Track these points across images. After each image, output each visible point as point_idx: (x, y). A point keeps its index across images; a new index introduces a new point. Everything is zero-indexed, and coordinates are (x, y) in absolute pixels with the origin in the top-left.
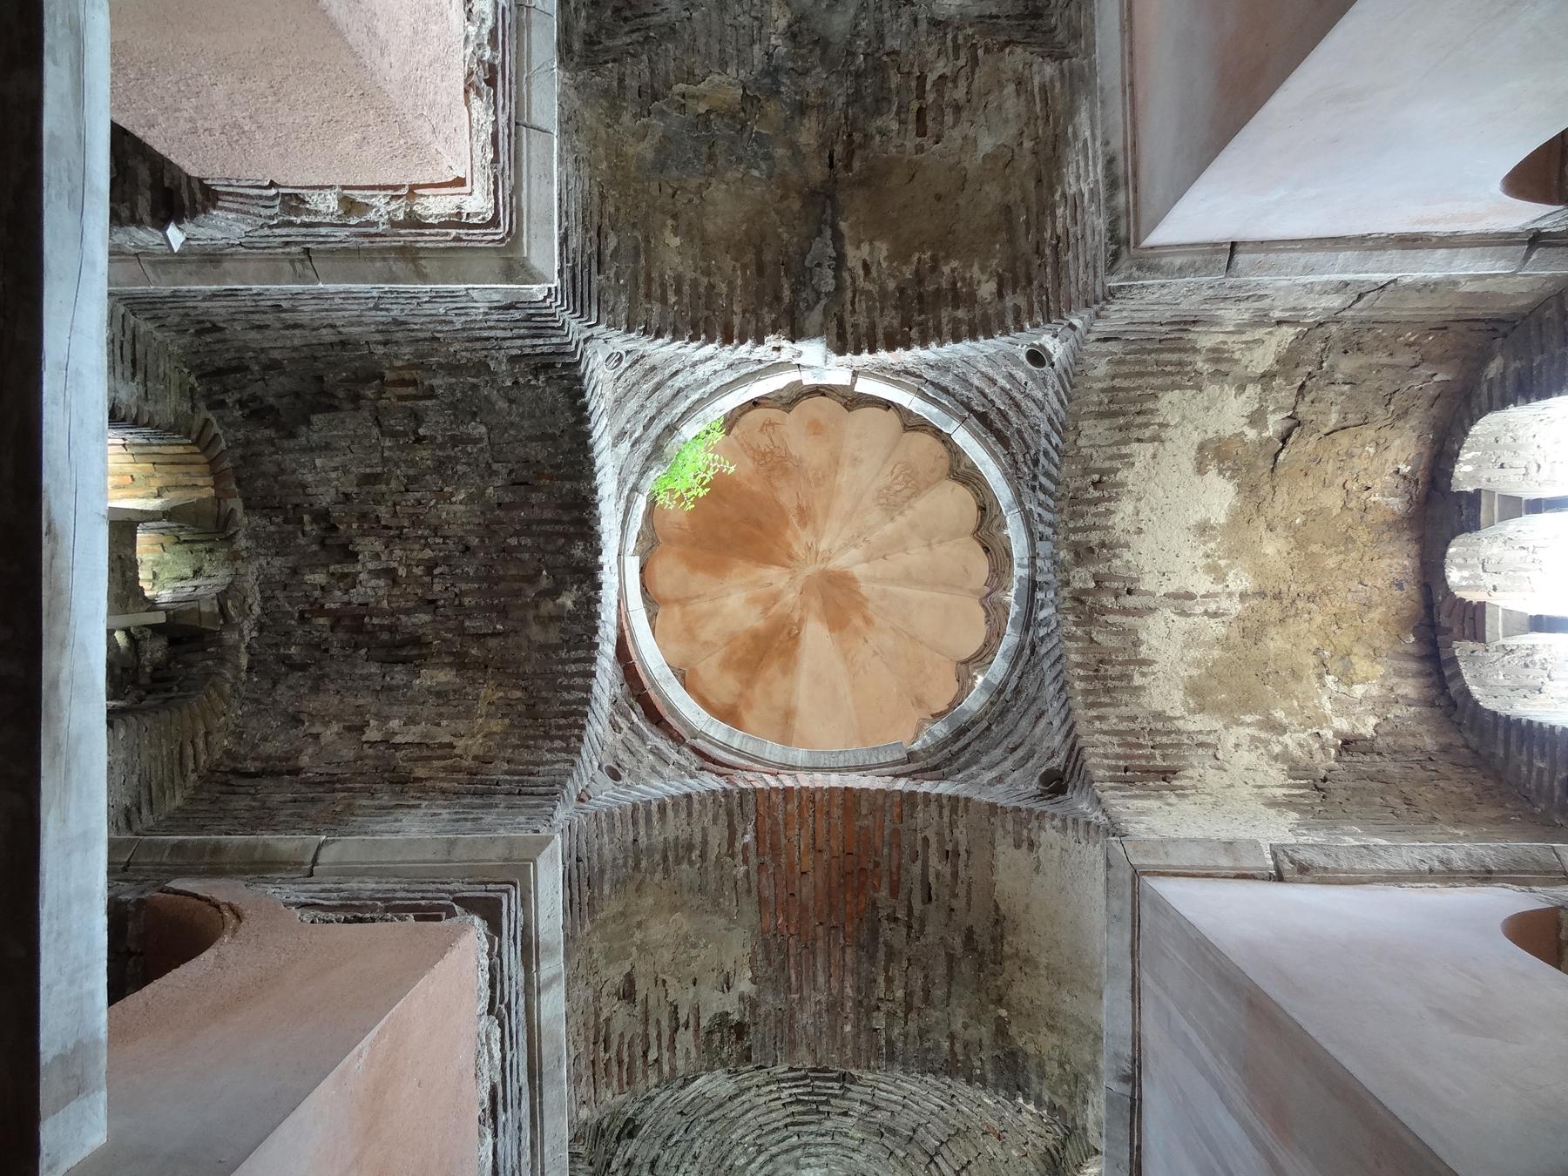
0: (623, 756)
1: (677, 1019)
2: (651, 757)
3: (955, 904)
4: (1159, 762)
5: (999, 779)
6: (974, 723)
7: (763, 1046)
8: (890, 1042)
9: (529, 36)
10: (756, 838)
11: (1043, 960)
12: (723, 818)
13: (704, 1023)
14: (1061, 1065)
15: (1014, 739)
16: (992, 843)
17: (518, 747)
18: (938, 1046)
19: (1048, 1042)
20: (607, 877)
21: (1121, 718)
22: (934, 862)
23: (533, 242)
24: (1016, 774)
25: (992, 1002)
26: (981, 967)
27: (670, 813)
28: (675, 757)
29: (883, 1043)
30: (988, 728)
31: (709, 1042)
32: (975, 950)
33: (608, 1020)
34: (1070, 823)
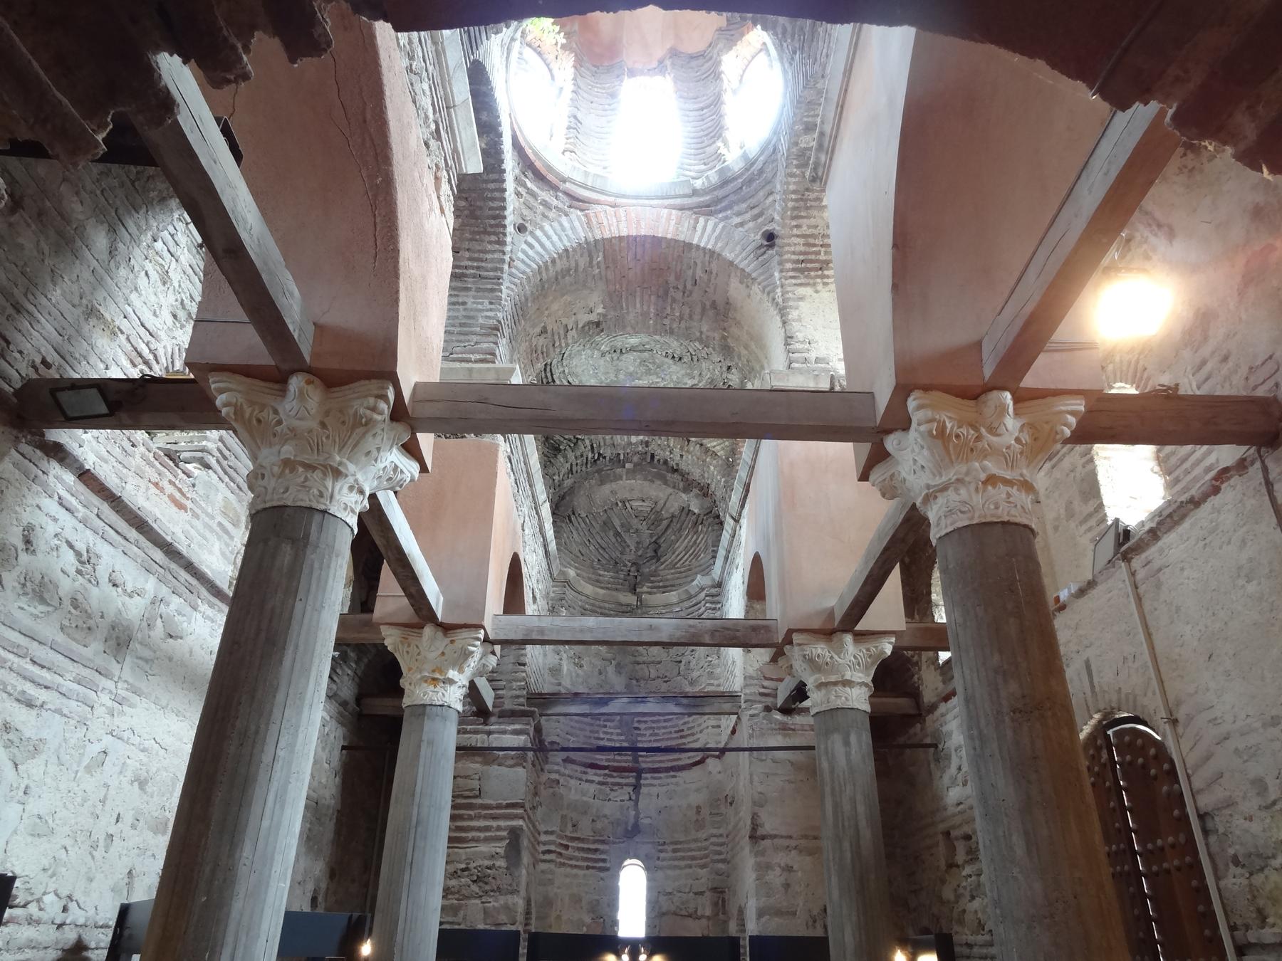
0: (526, 212)
2: (541, 207)
3: (707, 290)
4: (822, 257)
5: (742, 224)
6: (735, 179)
7: (609, 328)
9: (445, 57)
10: (604, 257)
11: (746, 328)
12: (586, 255)
13: (580, 326)
14: (748, 361)
15: (752, 201)
16: (729, 276)
17: (471, 240)
19: (744, 352)
20: (530, 299)
21: (809, 227)
22: (699, 273)
23: (468, 163)
24: (751, 224)
26: (717, 314)
27: (558, 261)
28: (555, 202)
30: (741, 188)
32: (716, 308)
34: (769, 291)
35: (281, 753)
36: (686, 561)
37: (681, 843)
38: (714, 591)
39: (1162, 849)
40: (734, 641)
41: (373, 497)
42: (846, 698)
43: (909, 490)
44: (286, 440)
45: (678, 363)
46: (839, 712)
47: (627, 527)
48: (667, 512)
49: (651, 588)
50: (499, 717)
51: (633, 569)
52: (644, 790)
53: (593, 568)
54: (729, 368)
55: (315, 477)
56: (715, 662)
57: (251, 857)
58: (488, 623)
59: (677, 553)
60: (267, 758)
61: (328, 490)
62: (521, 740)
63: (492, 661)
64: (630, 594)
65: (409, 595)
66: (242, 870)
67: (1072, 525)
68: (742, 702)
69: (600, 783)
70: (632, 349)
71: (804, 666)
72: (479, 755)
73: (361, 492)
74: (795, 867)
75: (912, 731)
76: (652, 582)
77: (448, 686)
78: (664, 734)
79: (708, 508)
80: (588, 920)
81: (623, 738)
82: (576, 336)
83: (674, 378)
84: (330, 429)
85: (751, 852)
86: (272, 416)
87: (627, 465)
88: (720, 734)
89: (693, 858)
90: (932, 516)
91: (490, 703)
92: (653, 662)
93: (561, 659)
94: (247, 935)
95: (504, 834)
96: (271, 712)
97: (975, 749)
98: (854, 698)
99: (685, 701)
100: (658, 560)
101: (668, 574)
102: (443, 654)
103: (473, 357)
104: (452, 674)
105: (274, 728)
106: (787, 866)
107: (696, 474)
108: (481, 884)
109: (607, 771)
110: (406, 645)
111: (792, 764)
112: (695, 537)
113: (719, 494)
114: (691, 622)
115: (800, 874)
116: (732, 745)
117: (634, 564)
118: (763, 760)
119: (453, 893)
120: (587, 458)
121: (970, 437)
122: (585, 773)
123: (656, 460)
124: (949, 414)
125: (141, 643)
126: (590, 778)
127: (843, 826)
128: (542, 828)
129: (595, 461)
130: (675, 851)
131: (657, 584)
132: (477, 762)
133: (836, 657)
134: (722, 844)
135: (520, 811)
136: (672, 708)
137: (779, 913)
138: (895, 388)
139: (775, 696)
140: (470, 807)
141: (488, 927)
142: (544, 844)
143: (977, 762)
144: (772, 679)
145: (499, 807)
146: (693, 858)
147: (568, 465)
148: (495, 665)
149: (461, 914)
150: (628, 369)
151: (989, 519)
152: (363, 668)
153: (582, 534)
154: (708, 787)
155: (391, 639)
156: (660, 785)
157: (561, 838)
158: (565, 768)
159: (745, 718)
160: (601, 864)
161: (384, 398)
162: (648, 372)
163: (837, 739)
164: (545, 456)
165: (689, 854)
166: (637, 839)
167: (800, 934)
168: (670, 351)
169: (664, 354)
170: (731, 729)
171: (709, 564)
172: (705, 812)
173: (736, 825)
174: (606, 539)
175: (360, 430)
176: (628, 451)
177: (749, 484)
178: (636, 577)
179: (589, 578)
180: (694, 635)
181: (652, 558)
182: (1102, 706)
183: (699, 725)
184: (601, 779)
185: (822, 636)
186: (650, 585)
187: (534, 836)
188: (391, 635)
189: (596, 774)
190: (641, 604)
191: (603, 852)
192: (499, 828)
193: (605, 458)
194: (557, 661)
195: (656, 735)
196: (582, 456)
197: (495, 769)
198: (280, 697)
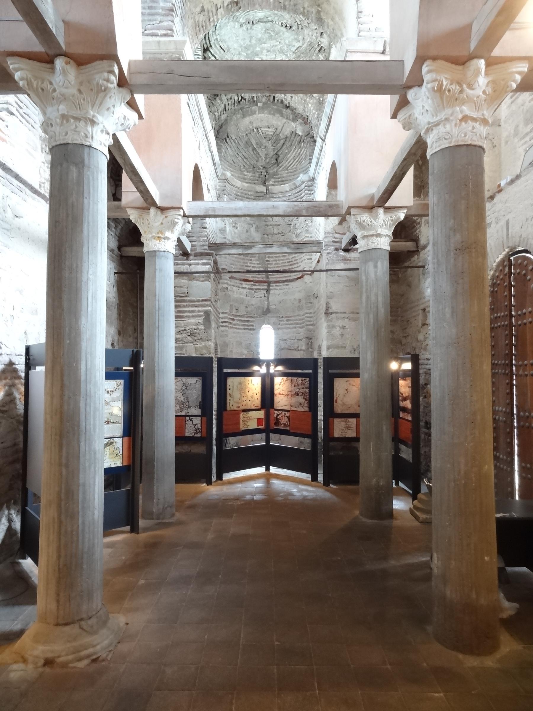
7: (244, 6)
8: (284, 5)
13: (226, 5)
14: (333, 30)
18: (300, 9)
19: (331, 23)
25: (317, 5)
29: (282, 6)
33: (198, 21)
35: (91, 277)
36: (294, 165)
37: (291, 317)
38: (310, 183)
39: (525, 314)
40: (319, 214)
41: (114, 136)
42: (377, 243)
43: (418, 125)
44: (61, 102)
45: (290, 31)
46: (373, 251)
47: (259, 145)
48: (283, 134)
49: (275, 182)
50: (194, 256)
51: (264, 171)
52: (272, 292)
53: (241, 171)
54: (322, 33)
55: (81, 125)
56: (310, 224)
57: (86, 324)
58: (184, 206)
59: (289, 161)
60: (84, 279)
61: (89, 133)
62: (207, 268)
63: (188, 227)
64: (262, 186)
65: (140, 192)
66: (83, 329)
67: (516, 140)
68: (323, 245)
69: (249, 289)
70: (260, 21)
71: (356, 226)
72: (186, 276)
73: (108, 133)
74: (347, 327)
75: (413, 259)
76: (275, 178)
77: (166, 240)
78: (282, 263)
79: (307, 132)
80: (245, 352)
81: (260, 266)
82: (223, 13)
83: (287, 42)
84: (85, 95)
85: (325, 320)
86: (49, 86)
87: (260, 104)
88: (312, 263)
89: (297, 324)
90: (429, 142)
91: (189, 249)
92: (276, 225)
93: (225, 224)
94: (91, 356)
95: (202, 314)
96: (82, 257)
97: (434, 269)
98: (382, 243)
99: (293, 246)
100: (278, 165)
101: (284, 174)
102: (162, 223)
103: (160, 32)
104: (168, 234)
105: (85, 265)
106: (343, 326)
107: (300, 109)
108: (192, 337)
109: (252, 283)
110: (142, 219)
111: (348, 277)
112: (299, 150)
113: (314, 122)
114: (296, 203)
115: (349, 330)
116: (318, 269)
117: (264, 167)
118: (332, 276)
119: (179, 341)
120: (234, 100)
121: (456, 91)
122: (241, 284)
123: (276, 100)
124: (446, 76)
125: (2, 221)
126: (244, 286)
127: (371, 307)
128: (220, 311)
129: (239, 102)
130: (287, 321)
131: (278, 180)
132: (185, 280)
133: (373, 221)
134: (311, 317)
135: (209, 303)
136: (286, 250)
137: (337, 347)
138: (416, 59)
139: (341, 243)
140: (184, 301)
141: (198, 355)
142: (222, 318)
143: (434, 276)
144: (340, 234)
145: (198, 301)
146: (297, 324)
147: (223, 105)
148: (190, 229)
149: (184, 350)
150: (257, 36)
151: (460, 143)
152: (119, 231)
153: (233, 150)
154: (305, 290)
155: (133, 216)
156: (280, 289)
157: (230, 315)
158: (230, 281)
159: (324, 255)
160: (251, 327)
161: (112, 72)
162: (271, 38)
163: (371, 265)
164: (209, 99)
165: (295, 322)
166: (268, 315)
167: (347, 356)
169: (280, 24)
170: (317, 260)
171: (307, 167)
172: (303, 302)
173: (318, 308)
174: (248, 152)
175: (101, 95)
178: (265, 175)
179: (239, 177)
180: (297, 211)
181: (274, 164)
182: (510, 245)
183: (301, 258)
184: (249, 287)
185: (367, 210)
186: (274, 180)
187: (217, 315)
188: (133, 214)
189: (247, 284)
190: (269, 192)
191: (252, 322)
192: (199, 311)
193: (245, 99)
194: (223, 226)
195: (278, 264)
196: (231, 99)
197: (194, 283)
198: (85, 249)
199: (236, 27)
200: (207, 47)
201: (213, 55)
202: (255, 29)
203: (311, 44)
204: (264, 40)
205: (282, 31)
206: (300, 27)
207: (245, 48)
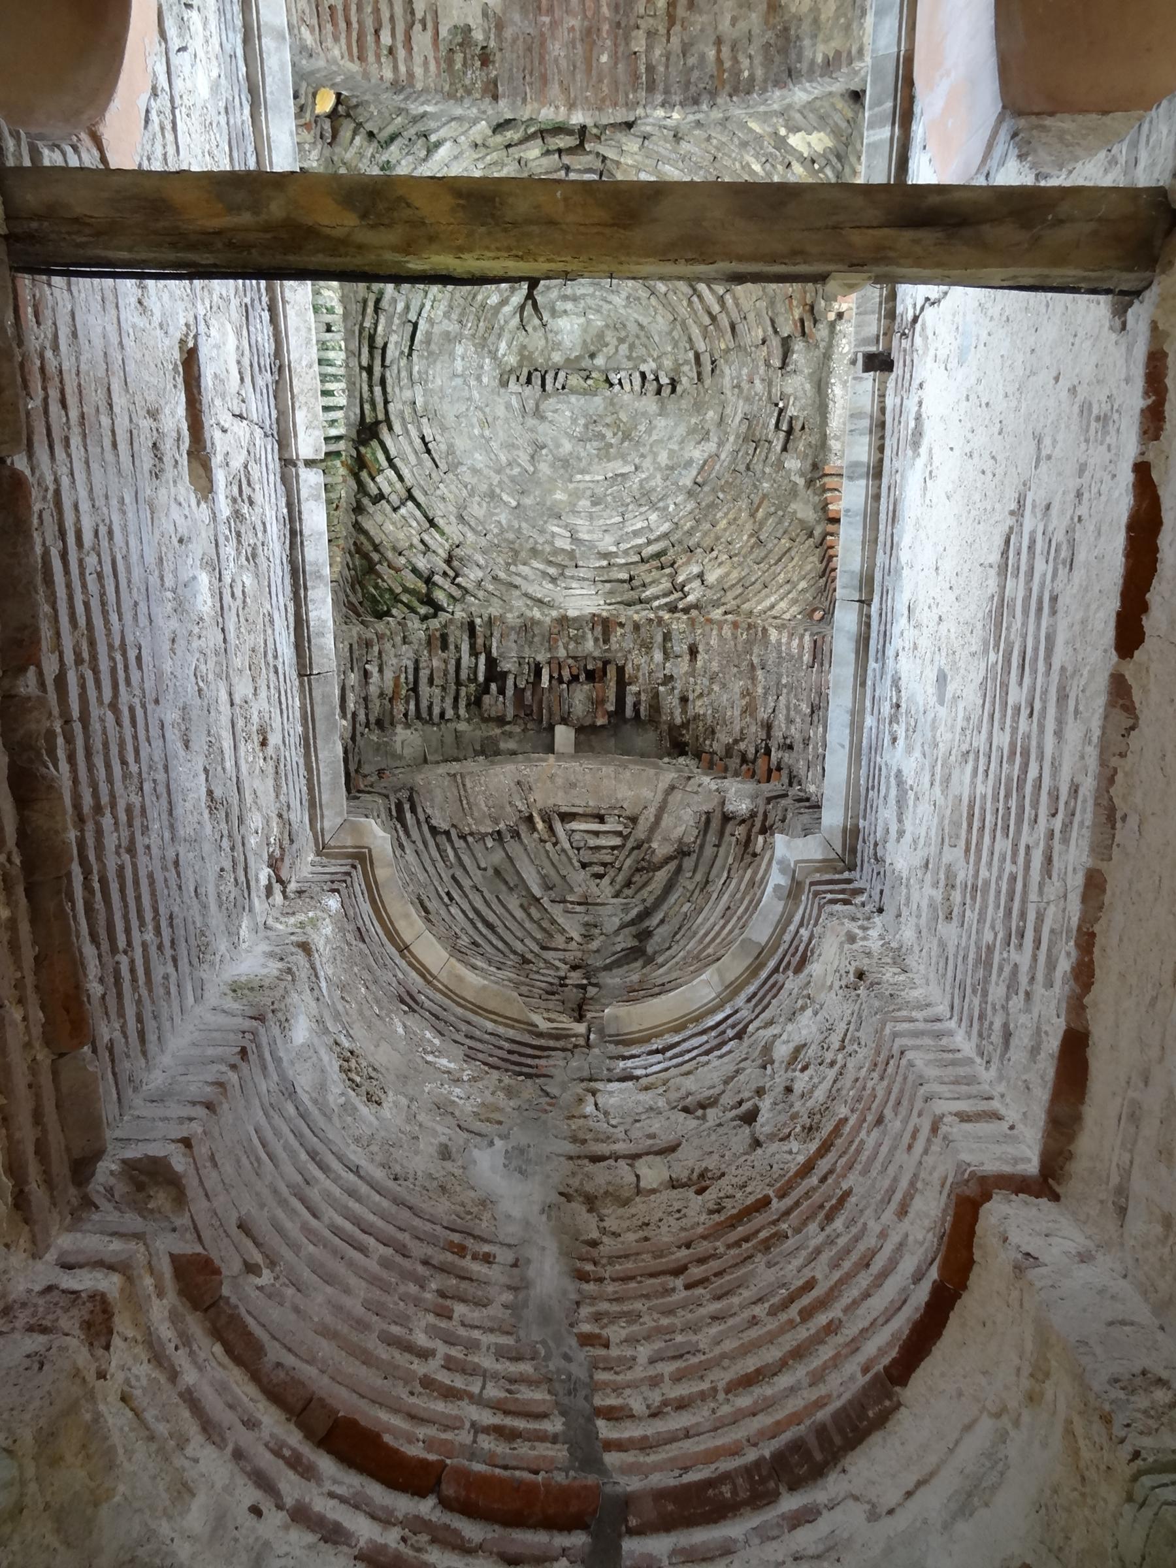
1: (413, 13)
7: (511, 78)
8: (650, 69)
18: (703, 57)
29: (643, 69)
31: (450, 62)
45: (671, 406)
109: (426, 1507)
122: (306, 1471)
150: (558, 446)
162: (605, 453)
168: (648, 367)
176: (562, 653)
177: (909, 60)
189: (356, 1503)
199: (485, 380)
200: (377, 423)
201: (392, 465)
202: (549, 415)
203: (752, 439)
204: (584, 463)
205: (644, 414)
206: (706, 359)
207: (513, 479)
